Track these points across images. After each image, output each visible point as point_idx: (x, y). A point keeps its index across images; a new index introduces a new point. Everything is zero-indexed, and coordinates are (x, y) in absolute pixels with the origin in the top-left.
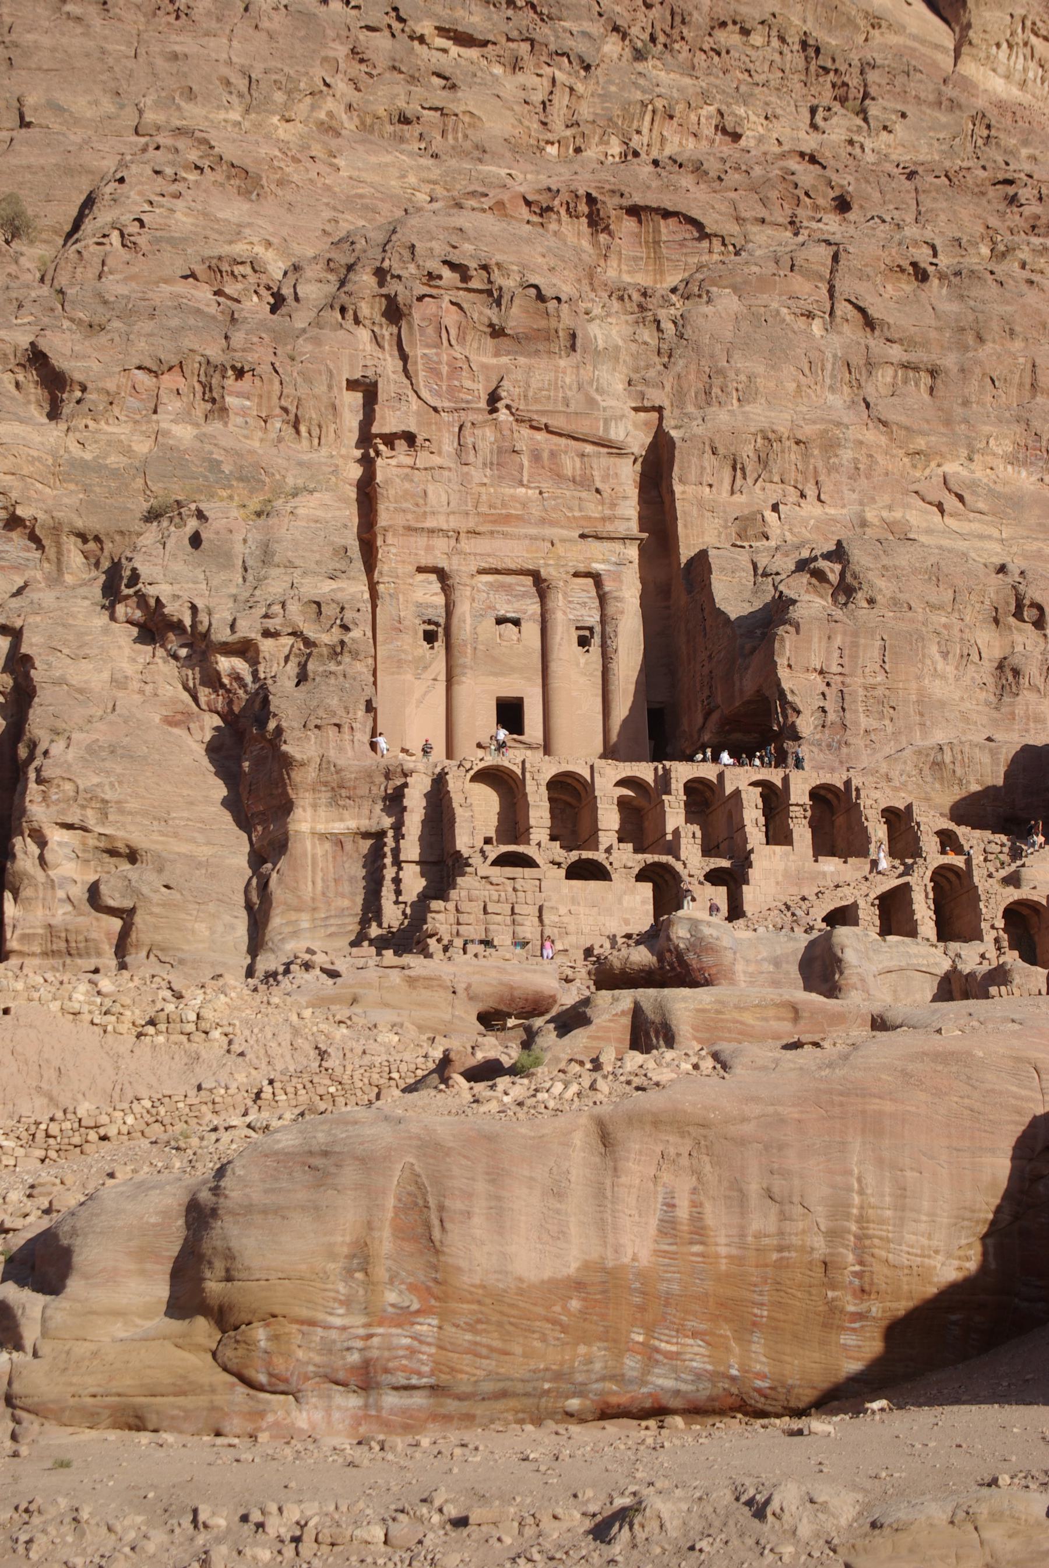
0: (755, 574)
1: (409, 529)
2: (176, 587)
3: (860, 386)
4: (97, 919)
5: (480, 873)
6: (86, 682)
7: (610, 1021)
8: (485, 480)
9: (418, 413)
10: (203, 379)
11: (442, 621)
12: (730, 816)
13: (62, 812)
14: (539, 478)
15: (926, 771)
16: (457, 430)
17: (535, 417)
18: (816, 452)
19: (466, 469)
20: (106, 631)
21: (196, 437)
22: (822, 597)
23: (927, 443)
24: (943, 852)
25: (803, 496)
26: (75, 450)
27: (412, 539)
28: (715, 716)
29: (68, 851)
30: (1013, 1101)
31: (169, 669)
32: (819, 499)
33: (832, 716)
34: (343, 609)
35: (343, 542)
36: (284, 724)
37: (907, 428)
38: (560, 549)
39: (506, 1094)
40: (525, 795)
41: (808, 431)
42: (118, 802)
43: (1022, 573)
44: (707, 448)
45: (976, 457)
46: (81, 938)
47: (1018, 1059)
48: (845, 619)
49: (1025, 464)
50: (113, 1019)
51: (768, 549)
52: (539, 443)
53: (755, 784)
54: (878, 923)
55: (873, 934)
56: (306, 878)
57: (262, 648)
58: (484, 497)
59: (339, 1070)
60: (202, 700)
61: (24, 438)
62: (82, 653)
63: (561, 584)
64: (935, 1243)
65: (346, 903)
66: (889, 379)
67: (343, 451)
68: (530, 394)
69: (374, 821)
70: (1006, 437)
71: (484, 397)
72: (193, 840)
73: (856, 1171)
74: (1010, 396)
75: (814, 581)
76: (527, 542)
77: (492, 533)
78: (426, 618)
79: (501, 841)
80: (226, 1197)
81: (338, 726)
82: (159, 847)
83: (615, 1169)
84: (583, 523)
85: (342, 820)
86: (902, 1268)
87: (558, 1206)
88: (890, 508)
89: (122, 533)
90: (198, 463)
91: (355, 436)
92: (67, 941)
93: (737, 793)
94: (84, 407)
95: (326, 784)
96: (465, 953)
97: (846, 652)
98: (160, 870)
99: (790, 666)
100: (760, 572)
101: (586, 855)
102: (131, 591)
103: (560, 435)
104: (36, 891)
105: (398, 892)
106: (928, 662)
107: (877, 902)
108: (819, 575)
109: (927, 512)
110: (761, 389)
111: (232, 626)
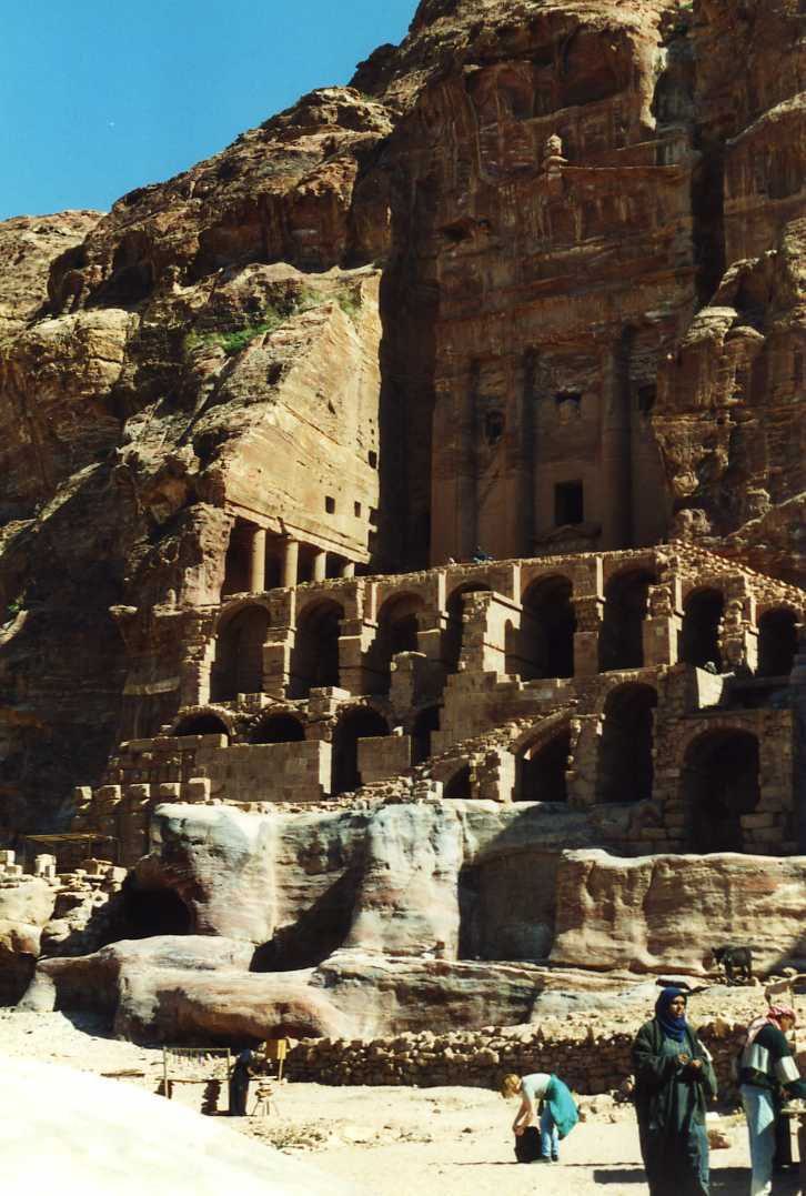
9: (477, 196)
57: (168, 494)
78: (489, 410)
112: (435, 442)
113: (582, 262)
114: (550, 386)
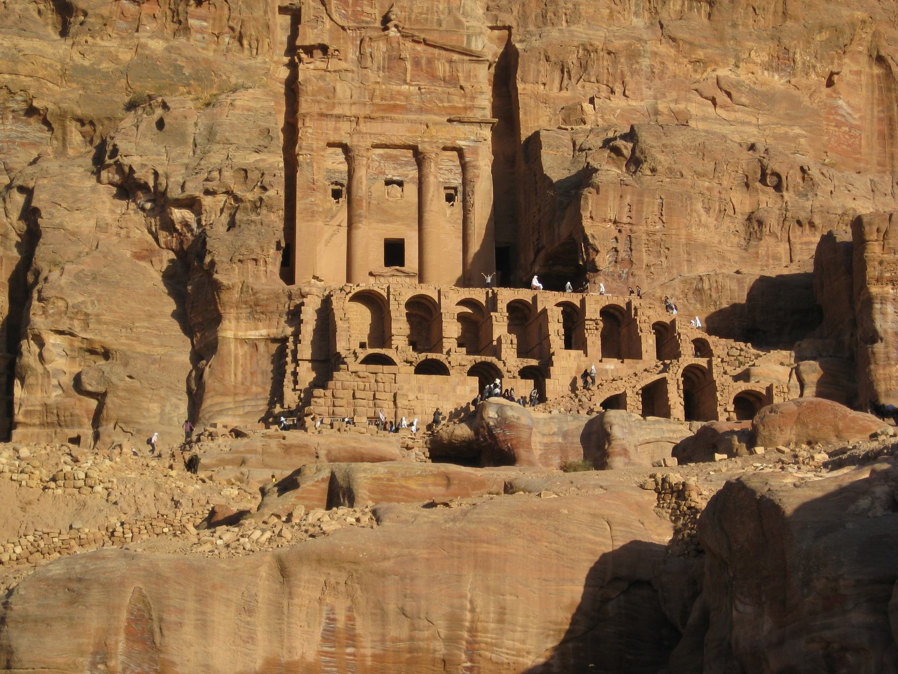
0: (574, 150)
1: (322, 115)
2: (145, 158)
3: (657, 13)
4: (80, 400)
5: (351, 368)
6: (77, 227)
7: (313, 485)
8: (379, 80)
9: (330, 31)
10: (172, 7)
11: (345, 183)
12: (540, 327)
13: (56, 322)
14: (419, 78)
15: (690, 295)
16: (359, 43)
17: (416, 33)
18: (623, 60)
19: (364, 71)
20: (94, 190)
21: (166, 49)
22: (618, 168)
23: (705, 54)
24: (696, 356)
25: (613, 92)
26: (77, 58)
27: (324, 123)
28: (542, 254)
29: (60, 350)
30: (589, 546)
31: (138, 218)
32: (624, 94)
33: (622, 254)
34: (263, 174)
35: (267, 125)
36: (216, 259)
37: (691, 44)
38: (433, 130)
39: (220, 538)
40: (389, 312)
41: (617, 44)
42: (97, 315)
43: (766, 150)
44: (542, 57)
45: (741, 65)
46: (67, 413)
47: (594, 516)
48: (634, 184)
49: (777, 70)
50: (26, 476)
51: (584, 131)
52: (419, 52)
53: (558, 305)
54: (641, 407)
55: (637, 415)
56: (230, 371)
57: (204, 203)
58: (377, 92)
59: (171, 516)
60: (162, 241)
61: (40, 51)
62: (75, 207)
64: (527, 647)
65: (259, 390)
66: (678, 8)
67: (276, 58)
68: (413, 17)
69: (281, 330)
70: (763, 50)
71: (379, 19)
72: (150, 343)
73: (469, 595)
74: (767, 20)
75: (613, 155)
76: (409, 125)
77: (383, 118)
78: (334, 180)
79: (371, 347)
80: (11, 609)
81: (256, 260)
82: (124, 348)
83: (290, 593)
84: (451, 111)
85: (257, 329)
86: (502, 664)
87: (249, 619)
88: (676, 101)
89: (109, 119)
90: (166, 68)
91: (285, 47)
92: (58, 415)
93: (545, 311)
94: (86, 27)
95: (246, 303)
96: (332, 428)
97: (634, 208)
98: (126, 365)
99: (591, 217)
100: (577, 148)
101: (431, 356)
102: (112, 161)
103: (435, 47)
104: (37, 379)
105: (296, 382)
106: (695, 215)
107: (640, 392)
108: (617, 151)
109: (704, 105)
110: (583, 14)
111: (183, 187)
112: (299, 194)
113: (407, 98)
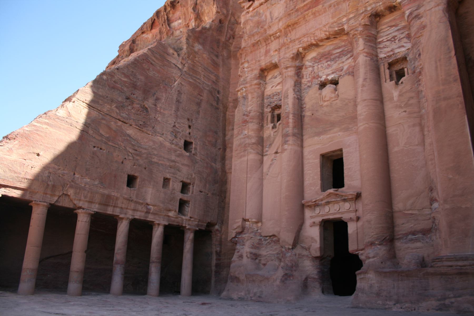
63: (360, 29)
76: (332, 10)
78: (273, 105)
114: (314, 78)
